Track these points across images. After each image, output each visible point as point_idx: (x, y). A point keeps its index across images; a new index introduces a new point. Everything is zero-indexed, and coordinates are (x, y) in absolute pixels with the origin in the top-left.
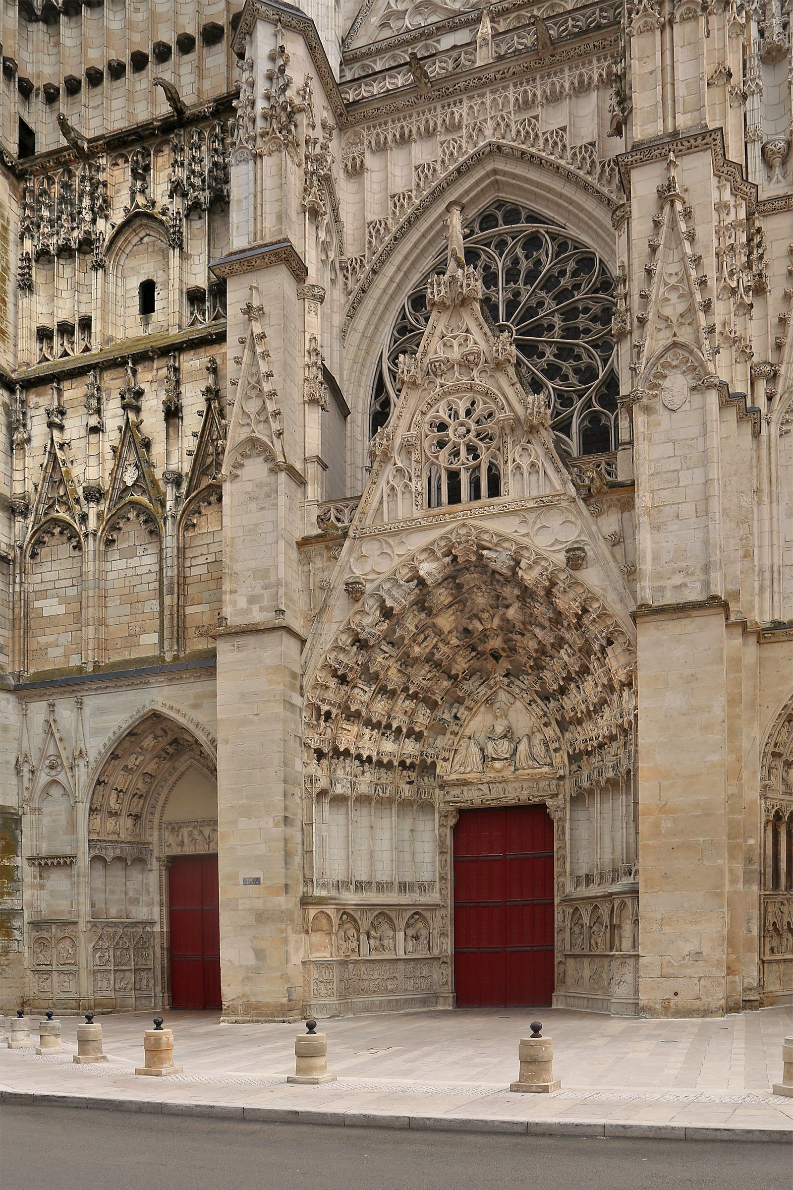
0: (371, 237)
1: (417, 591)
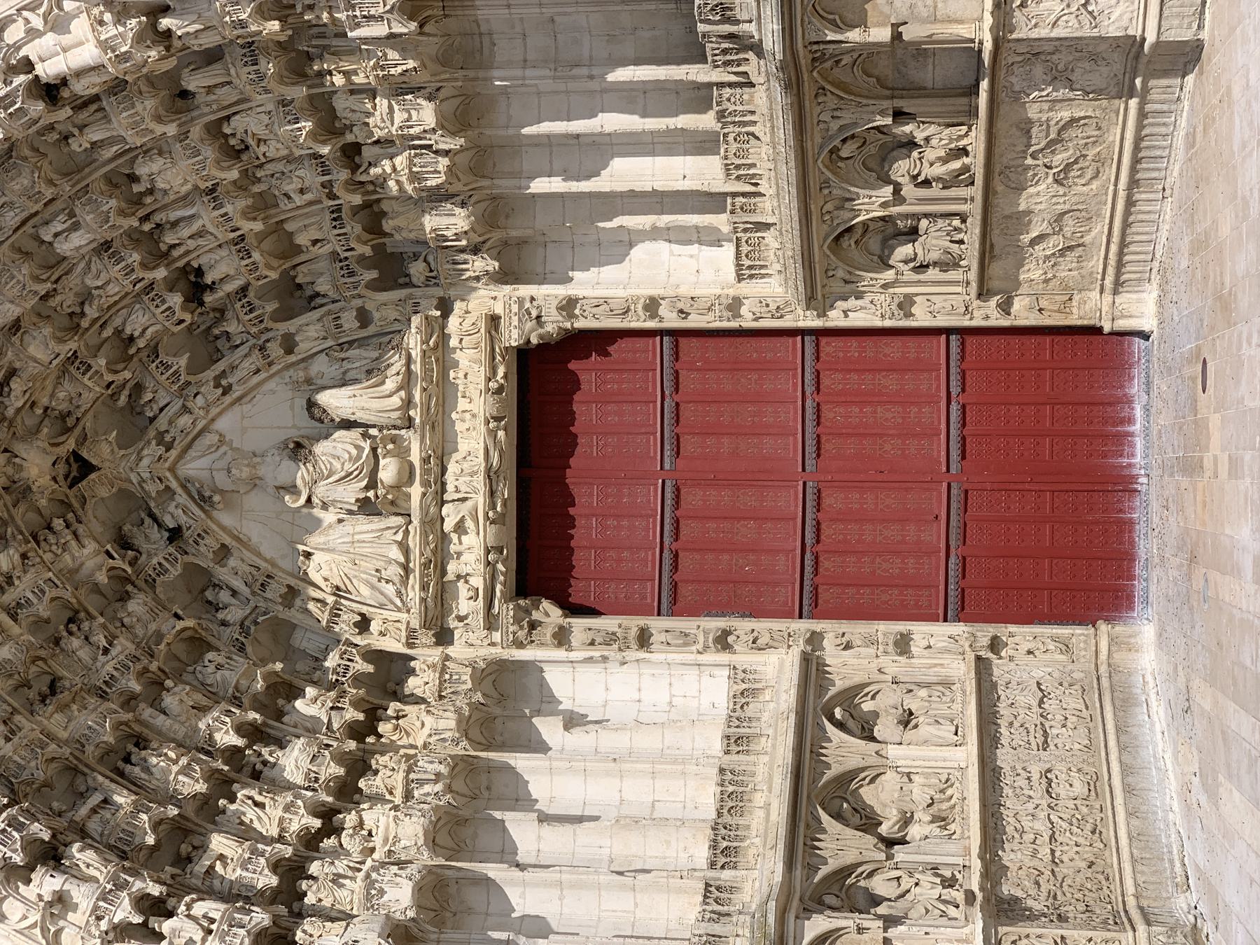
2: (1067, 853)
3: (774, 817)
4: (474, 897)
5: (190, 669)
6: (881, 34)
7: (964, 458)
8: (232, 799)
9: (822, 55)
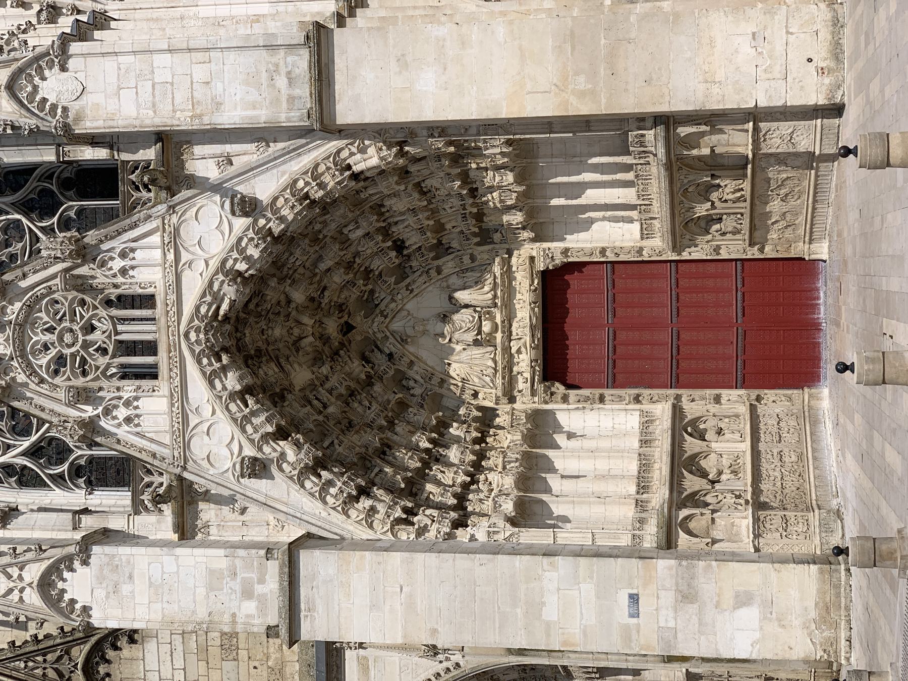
2: (787, 483)
3: (664, 473)
4: (537, 508)
5: (402, 415)
6: (706, 151)
7: (744, 316)
8: (431, 470)
9: (680, 159)
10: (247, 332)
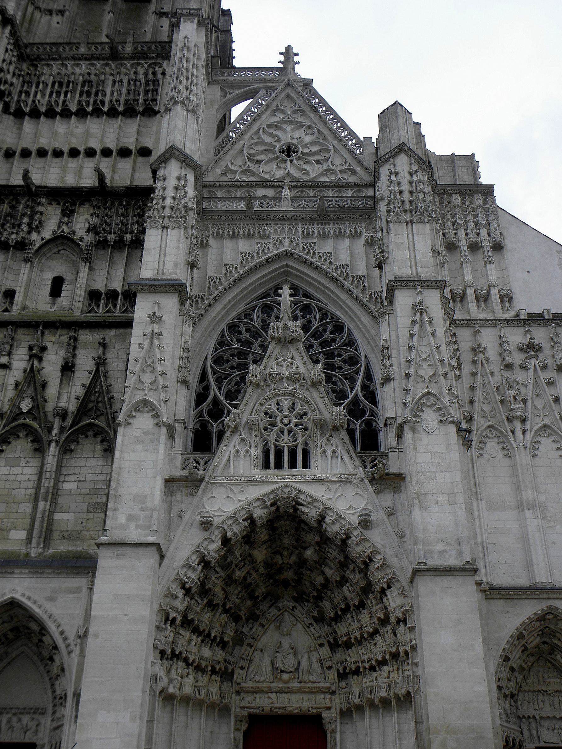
0: (210, 284)
1: (248, 528)
10: (288, 522)
